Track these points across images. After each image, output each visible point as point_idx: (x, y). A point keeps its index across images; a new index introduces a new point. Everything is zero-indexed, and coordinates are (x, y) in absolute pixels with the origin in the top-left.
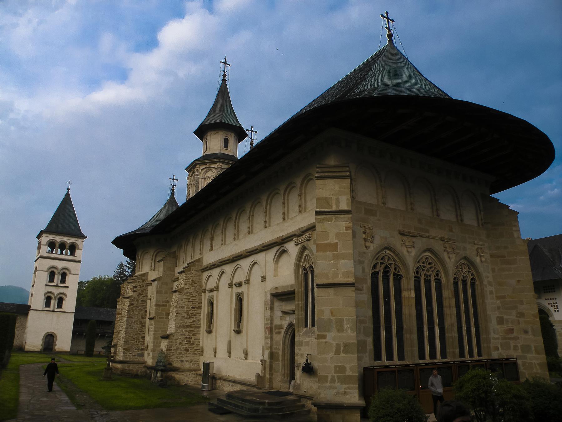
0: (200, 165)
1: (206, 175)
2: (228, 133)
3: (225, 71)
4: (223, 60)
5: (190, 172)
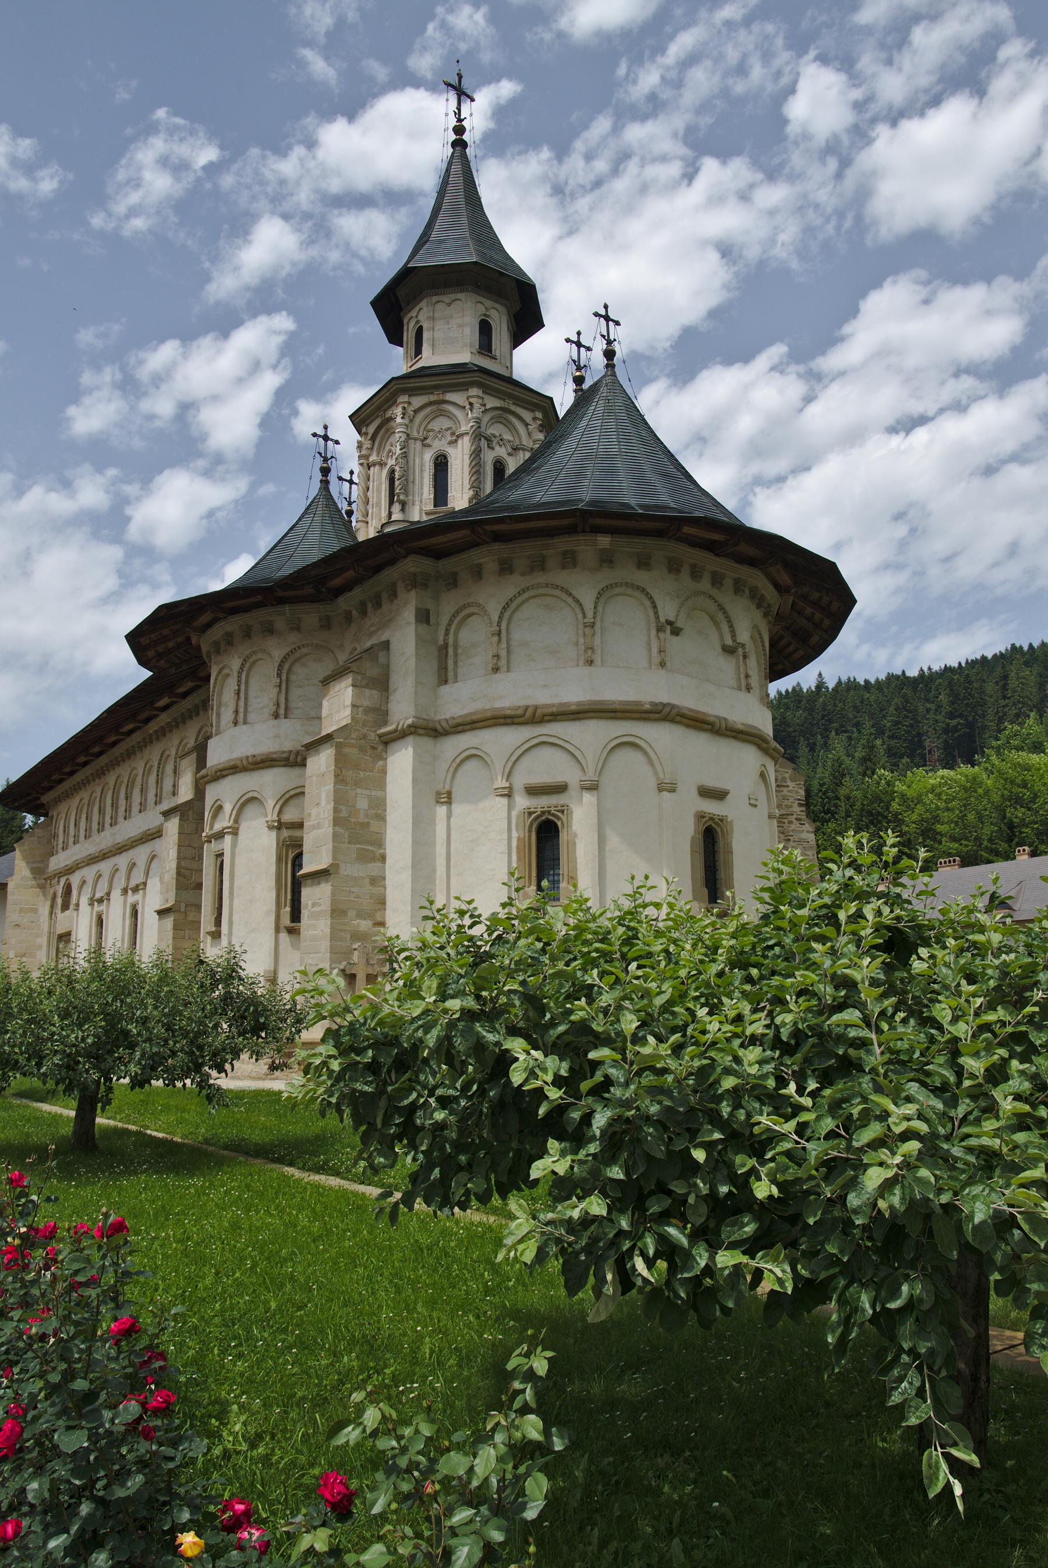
0: (410, 396)
1: (430, 427)
2: (488, 303)
3: (460, 115)
4: (454, 81)
5: (367, 426)
